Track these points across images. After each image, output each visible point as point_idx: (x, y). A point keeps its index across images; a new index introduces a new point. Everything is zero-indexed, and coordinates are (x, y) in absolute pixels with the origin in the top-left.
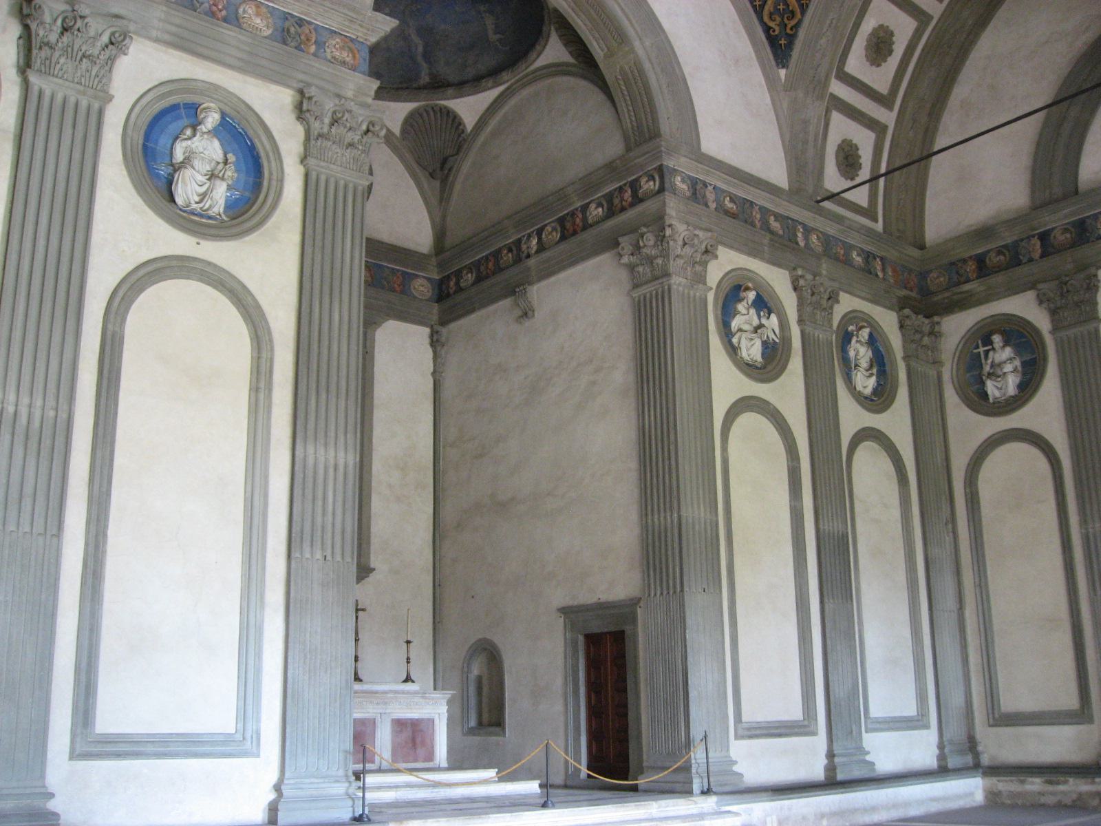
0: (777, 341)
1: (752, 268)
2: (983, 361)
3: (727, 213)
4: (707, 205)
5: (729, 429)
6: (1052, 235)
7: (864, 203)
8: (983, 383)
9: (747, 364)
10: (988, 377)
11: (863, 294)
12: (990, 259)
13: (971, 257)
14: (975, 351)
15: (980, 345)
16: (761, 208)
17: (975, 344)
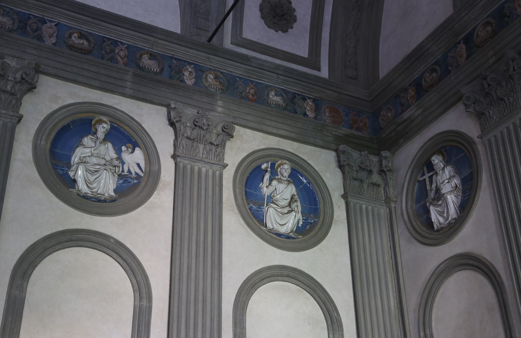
0: (142, 175)
1: (109, 103)
2: (428, 187)
3: (71, 47)
4: (40, 38)
5: (33, 265)
6: (475, 34)
7: (303, 52)
8: (428, 212)
9: (85, 197)
10: (431, 203)
11: (281, 132)
12: (425, 80)
13: (410, 85)
14: (421, 179)
15: (426, 172)
16: (128, 47)
17: (422, 172)
